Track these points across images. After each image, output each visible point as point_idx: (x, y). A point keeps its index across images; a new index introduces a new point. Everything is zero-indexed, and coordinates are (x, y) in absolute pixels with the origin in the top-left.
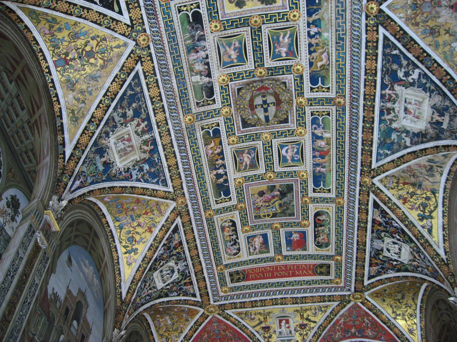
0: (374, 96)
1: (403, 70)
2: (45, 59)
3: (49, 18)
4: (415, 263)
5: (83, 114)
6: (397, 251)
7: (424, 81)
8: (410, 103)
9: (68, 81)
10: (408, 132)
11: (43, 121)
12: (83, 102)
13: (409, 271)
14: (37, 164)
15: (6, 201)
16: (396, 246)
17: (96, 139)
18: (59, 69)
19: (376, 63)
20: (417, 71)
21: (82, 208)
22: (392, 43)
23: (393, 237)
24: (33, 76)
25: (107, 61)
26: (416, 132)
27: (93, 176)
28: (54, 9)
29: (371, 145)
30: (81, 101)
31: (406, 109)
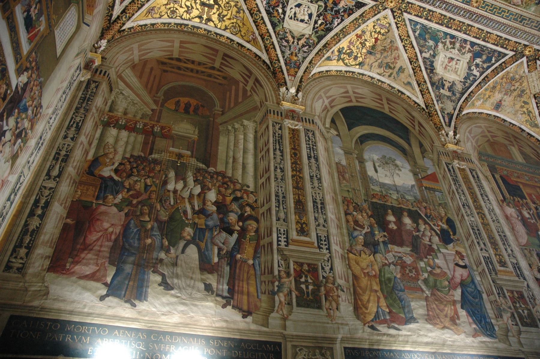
0: (468, 35)
1: (481, 63)
4: (291, 40)
6: (300, 17)
7: (471, 79)
8: (456, 64)
10: (434, 56)
13: (274, 28)
16: (306, 18)
19: (492, 44)
20: (478, 74)
22: (500, 59)
23: (318, 16)
26: (434, 64)
29: (427, 19)
31: (452, 59)
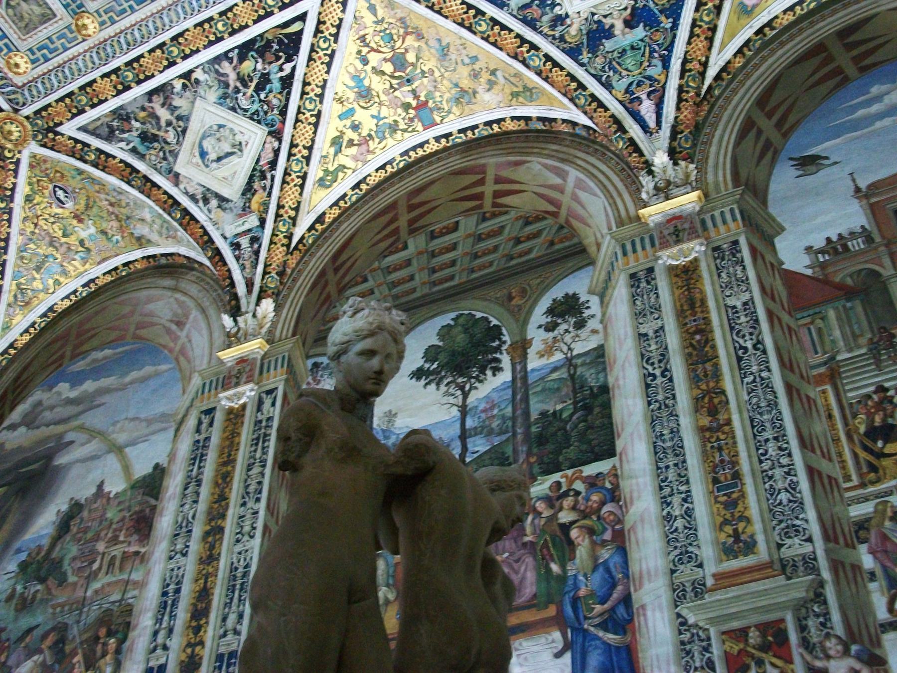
2: (421, 145)
3: (332, 151)
5: (516, 75)
9: (457, 101)
11: (505, 173)
12: (493, 73)
14: (555, 215)
15: (542, 330)
17: (563, 50)
18: (438, 119)
21: (748, 76)
24: (432, 182)
25: (406, 27)
27: (651, 56)
28: (310, 149)
30: (493, 78)
